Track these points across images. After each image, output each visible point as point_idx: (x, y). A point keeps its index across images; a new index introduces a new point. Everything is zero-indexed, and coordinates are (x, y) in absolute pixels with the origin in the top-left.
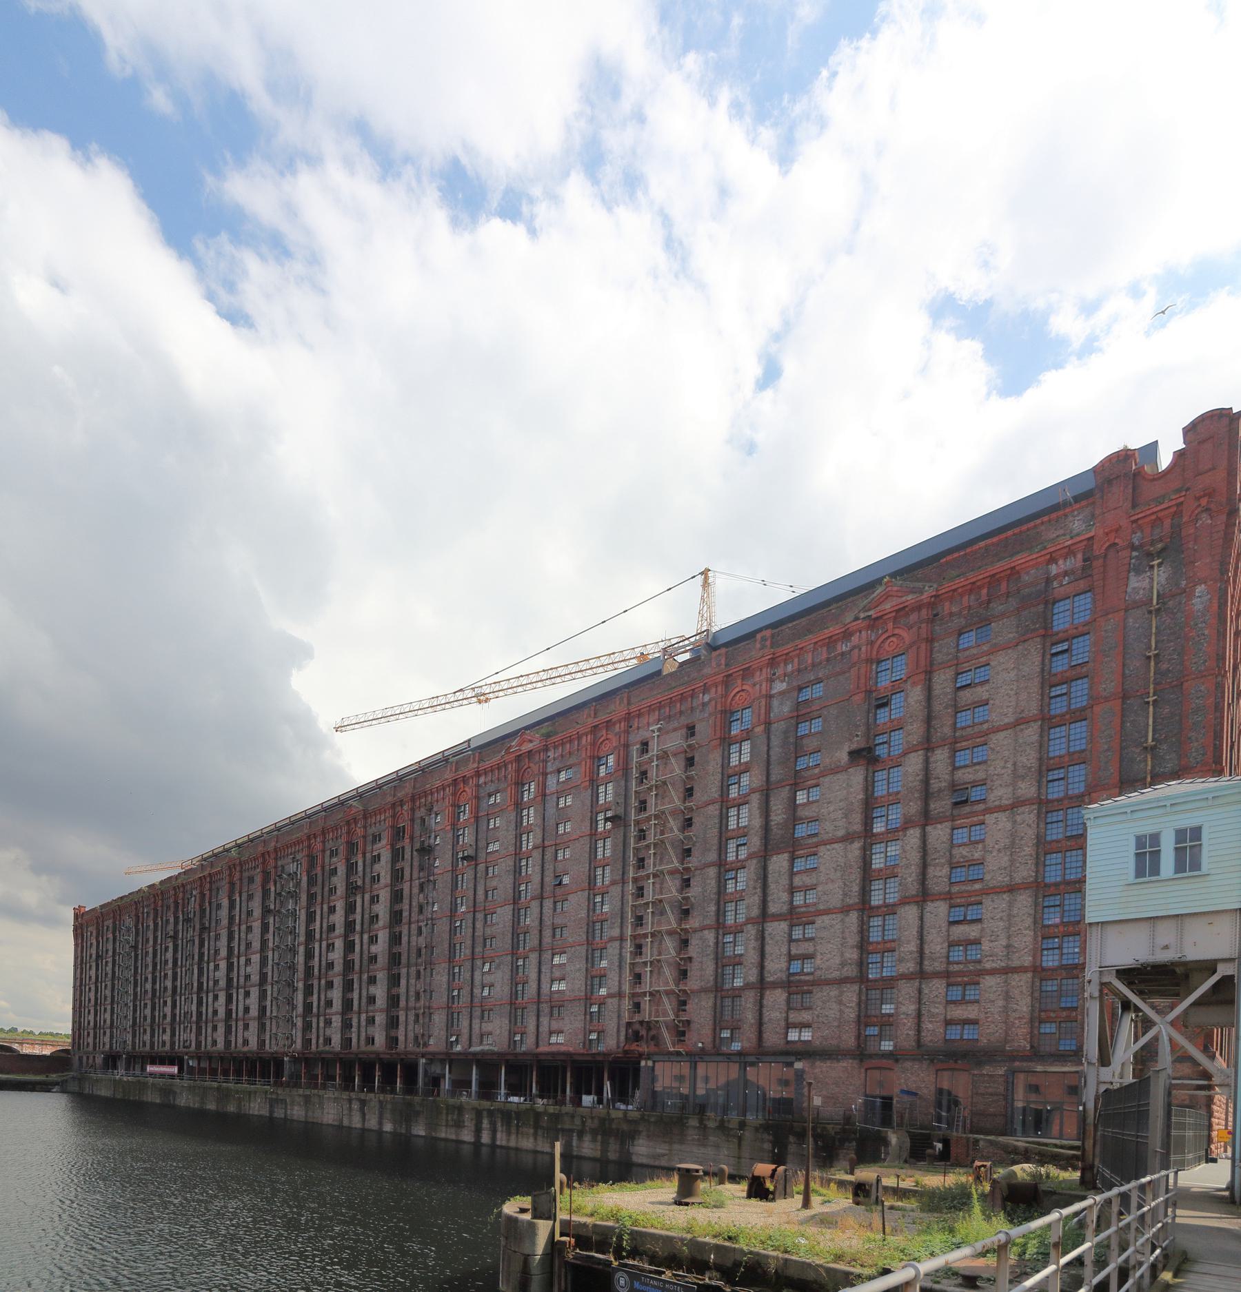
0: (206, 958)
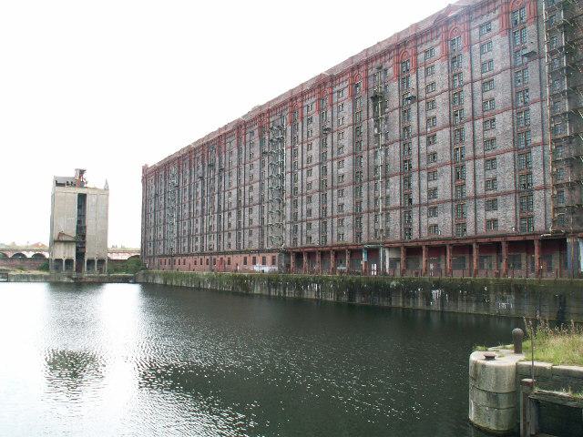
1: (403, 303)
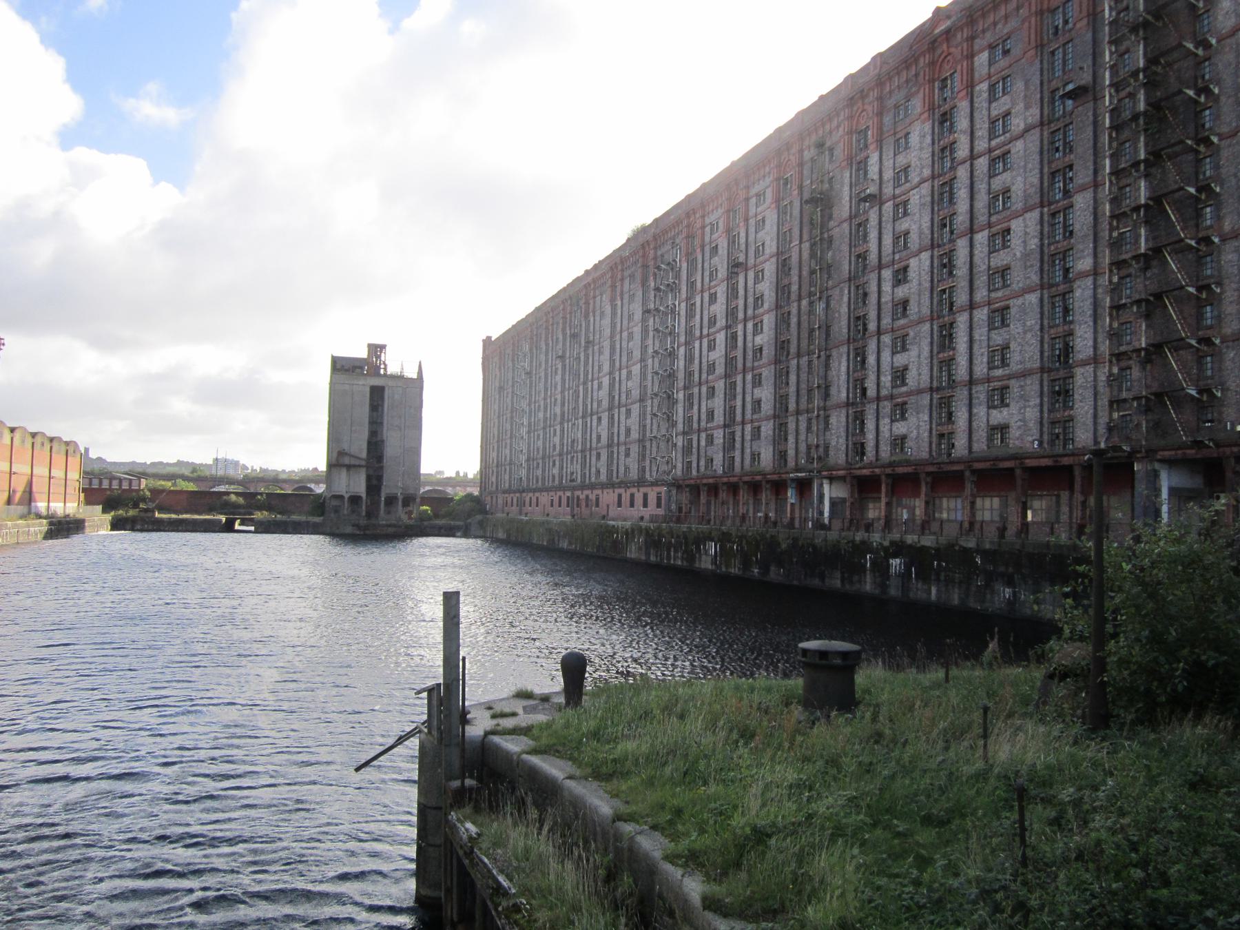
1: (842, 581)
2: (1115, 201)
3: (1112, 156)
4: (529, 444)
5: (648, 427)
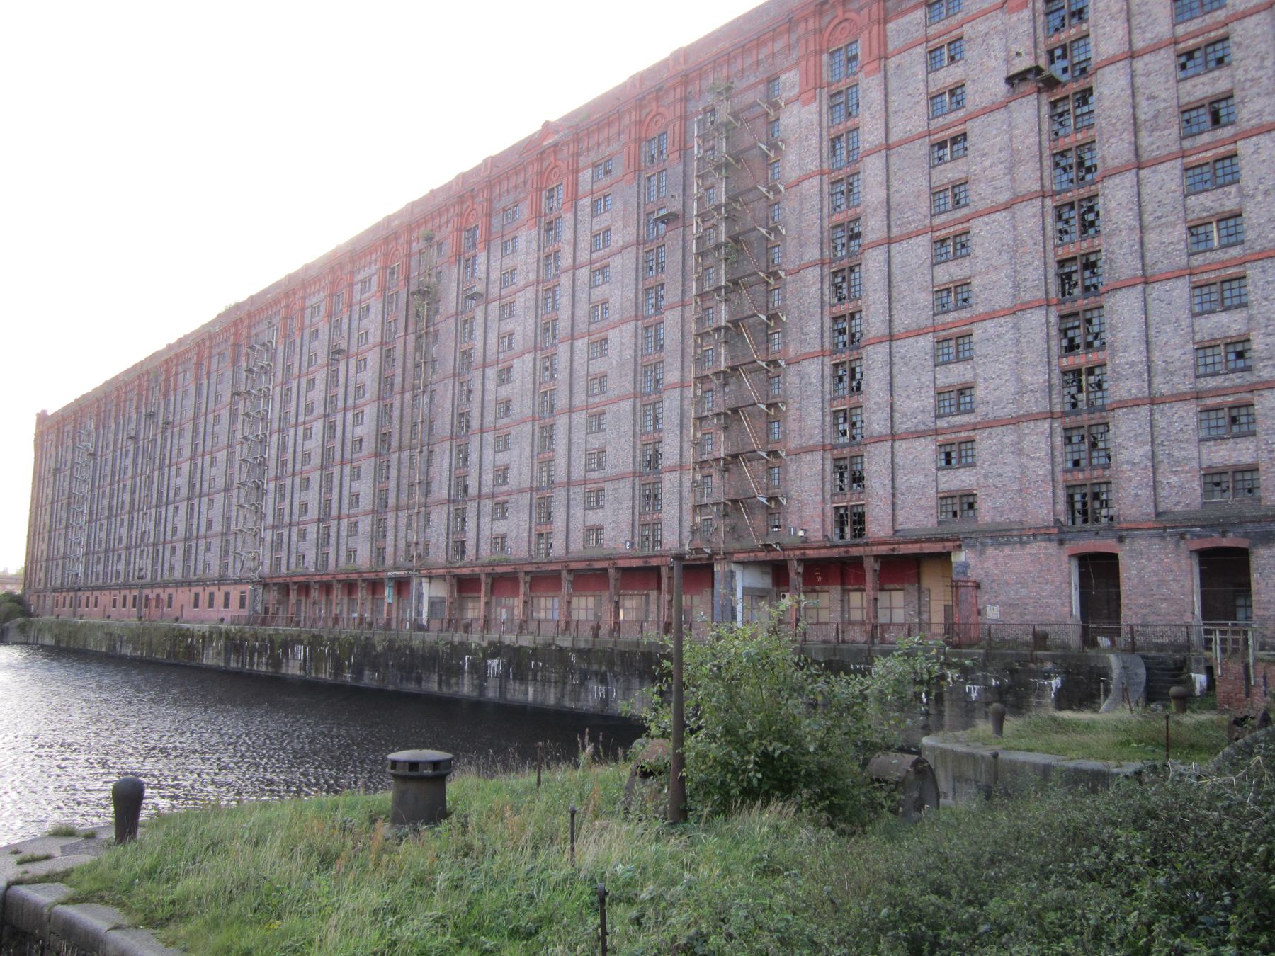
0: (167, 462)
1: (440, 684)
2: (699, 320)
3: (698, 279)
4: (89, 536)
5: (233, 519)
